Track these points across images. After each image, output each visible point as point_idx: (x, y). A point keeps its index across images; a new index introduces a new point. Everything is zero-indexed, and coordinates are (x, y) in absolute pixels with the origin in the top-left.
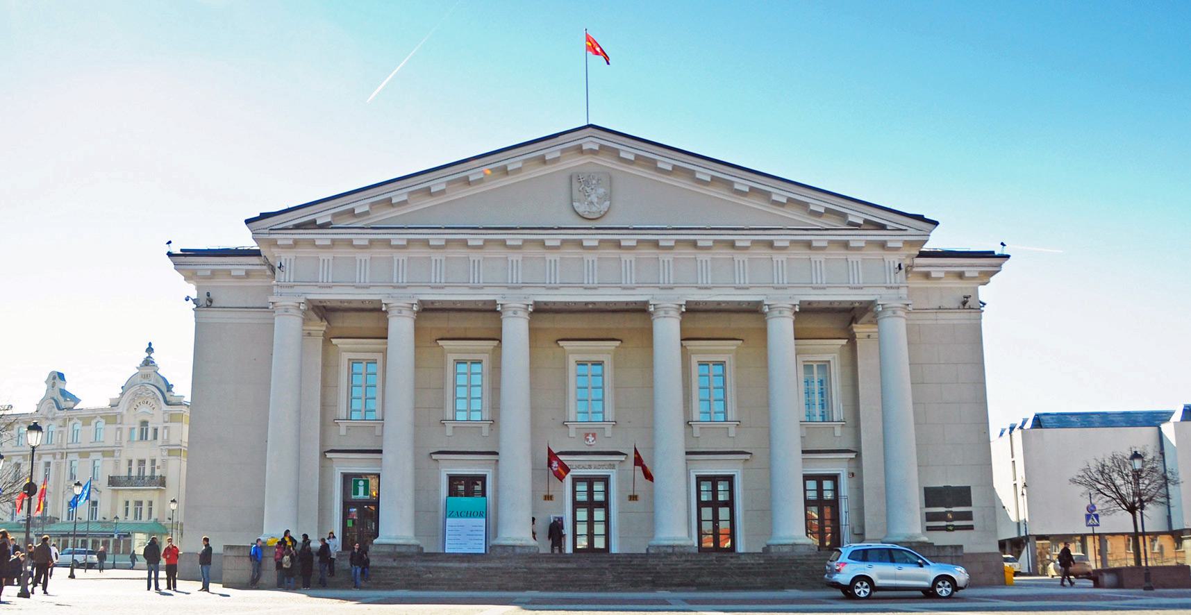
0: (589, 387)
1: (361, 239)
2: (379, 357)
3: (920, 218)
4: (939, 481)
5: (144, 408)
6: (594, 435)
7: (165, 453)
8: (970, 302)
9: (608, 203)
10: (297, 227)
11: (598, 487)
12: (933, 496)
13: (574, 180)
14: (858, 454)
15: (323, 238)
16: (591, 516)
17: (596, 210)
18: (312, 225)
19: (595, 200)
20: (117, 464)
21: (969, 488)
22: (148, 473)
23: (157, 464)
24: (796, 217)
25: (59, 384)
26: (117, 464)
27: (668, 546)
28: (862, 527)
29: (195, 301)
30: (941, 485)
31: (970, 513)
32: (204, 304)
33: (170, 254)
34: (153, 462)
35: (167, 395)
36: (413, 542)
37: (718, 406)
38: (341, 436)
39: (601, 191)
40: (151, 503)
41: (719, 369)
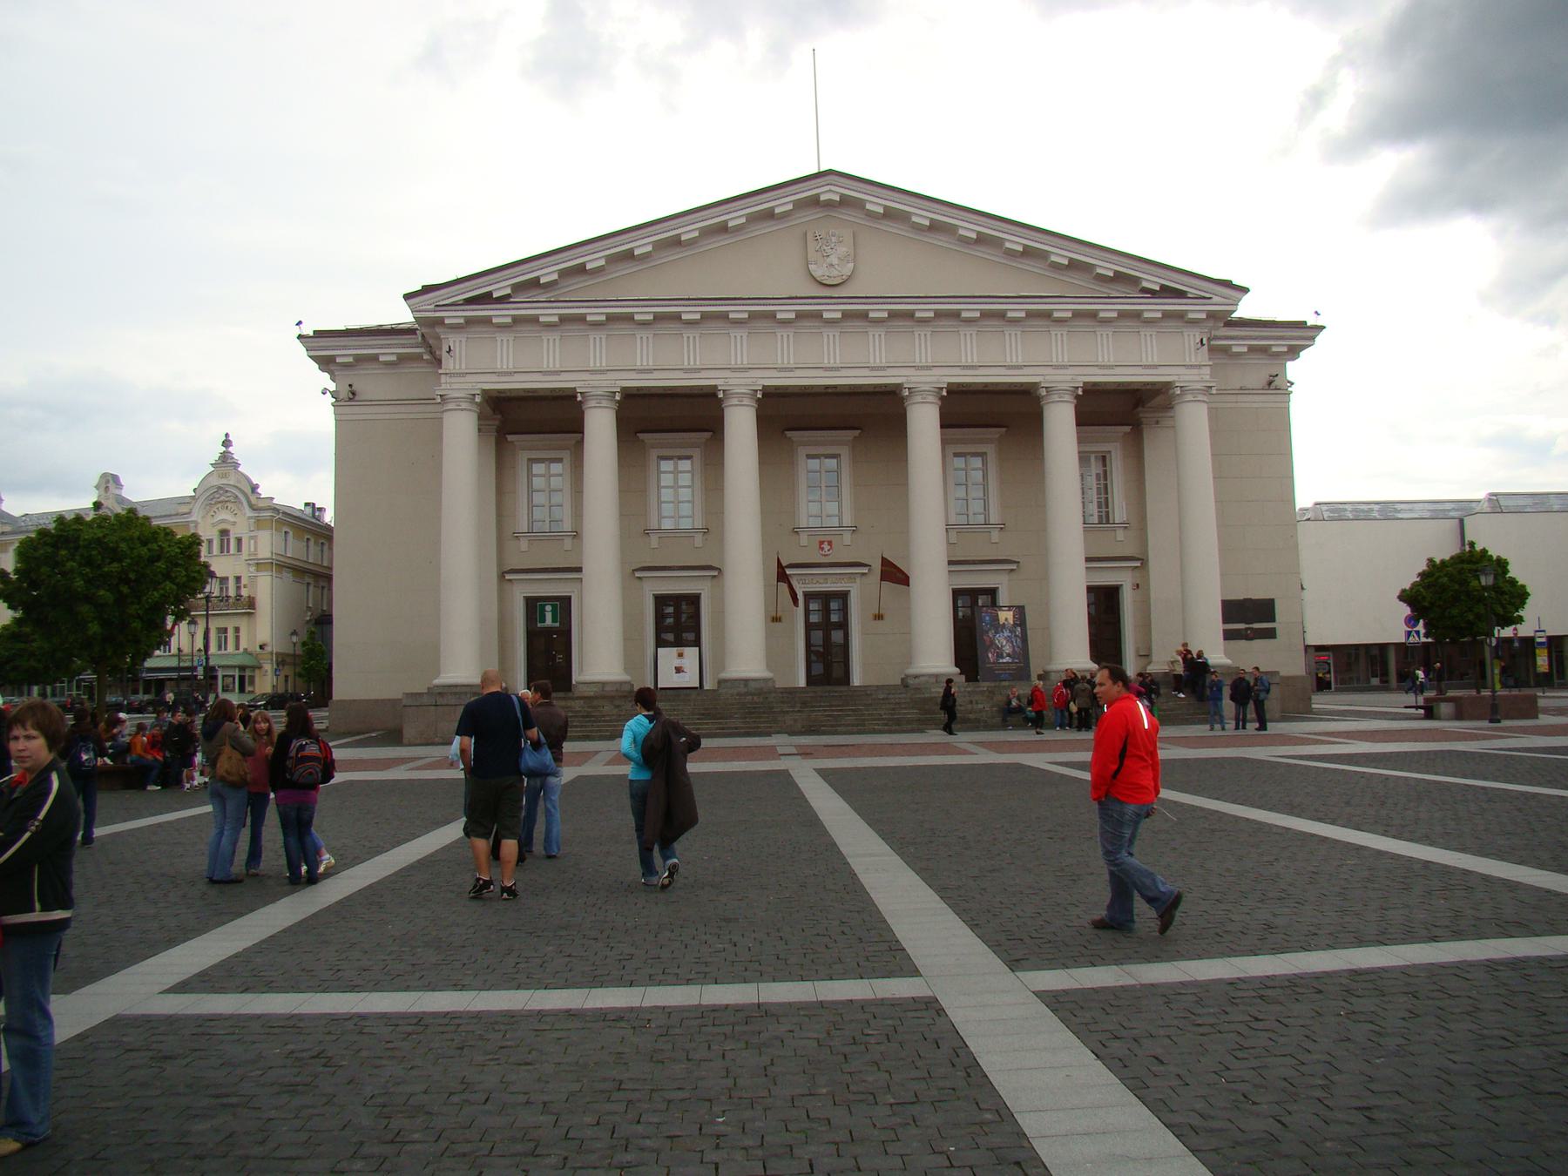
0: (827, 491)
1: (549, 314)
3: (1227, 284)
4: (1239, 595)
5: (224, 515)
6: (830, 543)
7: (253, 569)
8: (1277, 382)
9: (851, 265)
10: (469, 301)
11: (834, 605)
13: (810, 236)
14: (1144, 561)
15: (501, 315)
16: (827, 638)
17: (833, 276)
18: (486, 299)
19: (834, 260)
21: (1272, 601)
22: (232, 592)
23: (244, 581)
24: (1078, 280)
25: (113, 490)
27: (930, 676)
28: (1150, 649)
29: (334, 394)
31: (1274, 630)
32: (346, 399)
33: (300, 337)
34: (238, 579)
35: (253, 499)
36: (626, 678)
37: (977, 506)
38: (523, 553)
39: (842, 250)
40: (237, 630)
41: (977, 462)
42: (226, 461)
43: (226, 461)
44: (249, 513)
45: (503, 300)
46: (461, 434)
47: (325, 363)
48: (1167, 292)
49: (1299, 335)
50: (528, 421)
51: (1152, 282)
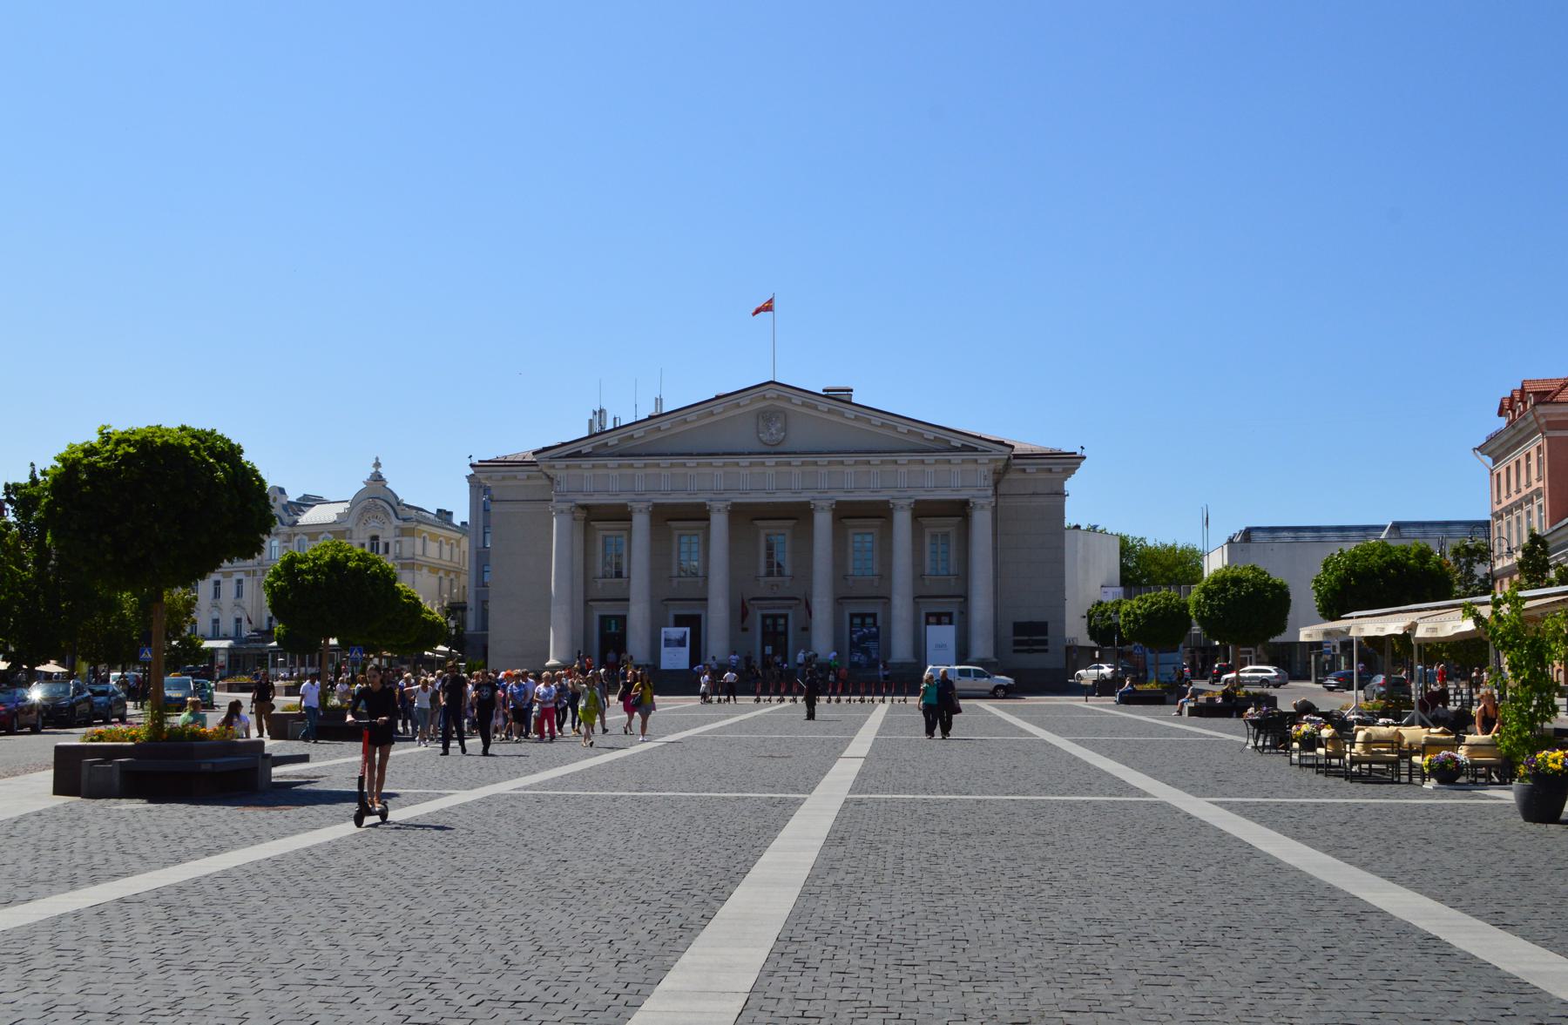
2: (625, 533)
3: (1001, 443)
4: (1024, 617)
10: (568, 456)
11: (782, 621)
12: (1019, 628)
18: (578, 455)
30: (1026, 620)
42: (377, 478)
43: (377, 478)
44: (396, 522)
45: (588, 455)
48: (965, 448)
49: (1069, 462)
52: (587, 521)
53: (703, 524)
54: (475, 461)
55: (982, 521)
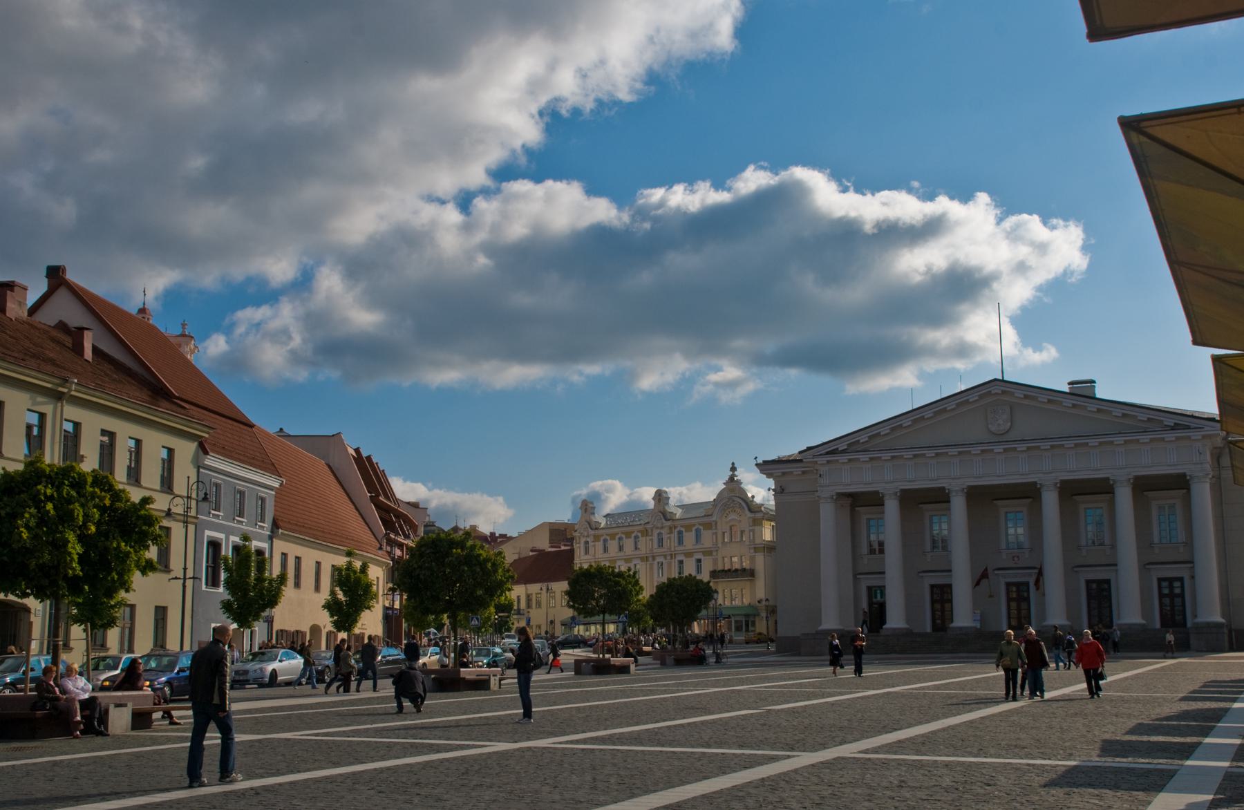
1: (864, 457)
5: (733, 516)
10: (828, 453)
15: (844, 458)
19: (1001, 422)
20: (715, 561)
26: (715, 561)
44: (749, 515)
45: (844, 451)
46: (827, 513)
47: (769, 476)
48: (1176, 427)
50: (860, 503)
51: (1170, 422)
52: (853, 507)
53: (945, 505)
54: (760, 461)
55: (1203, 494)
